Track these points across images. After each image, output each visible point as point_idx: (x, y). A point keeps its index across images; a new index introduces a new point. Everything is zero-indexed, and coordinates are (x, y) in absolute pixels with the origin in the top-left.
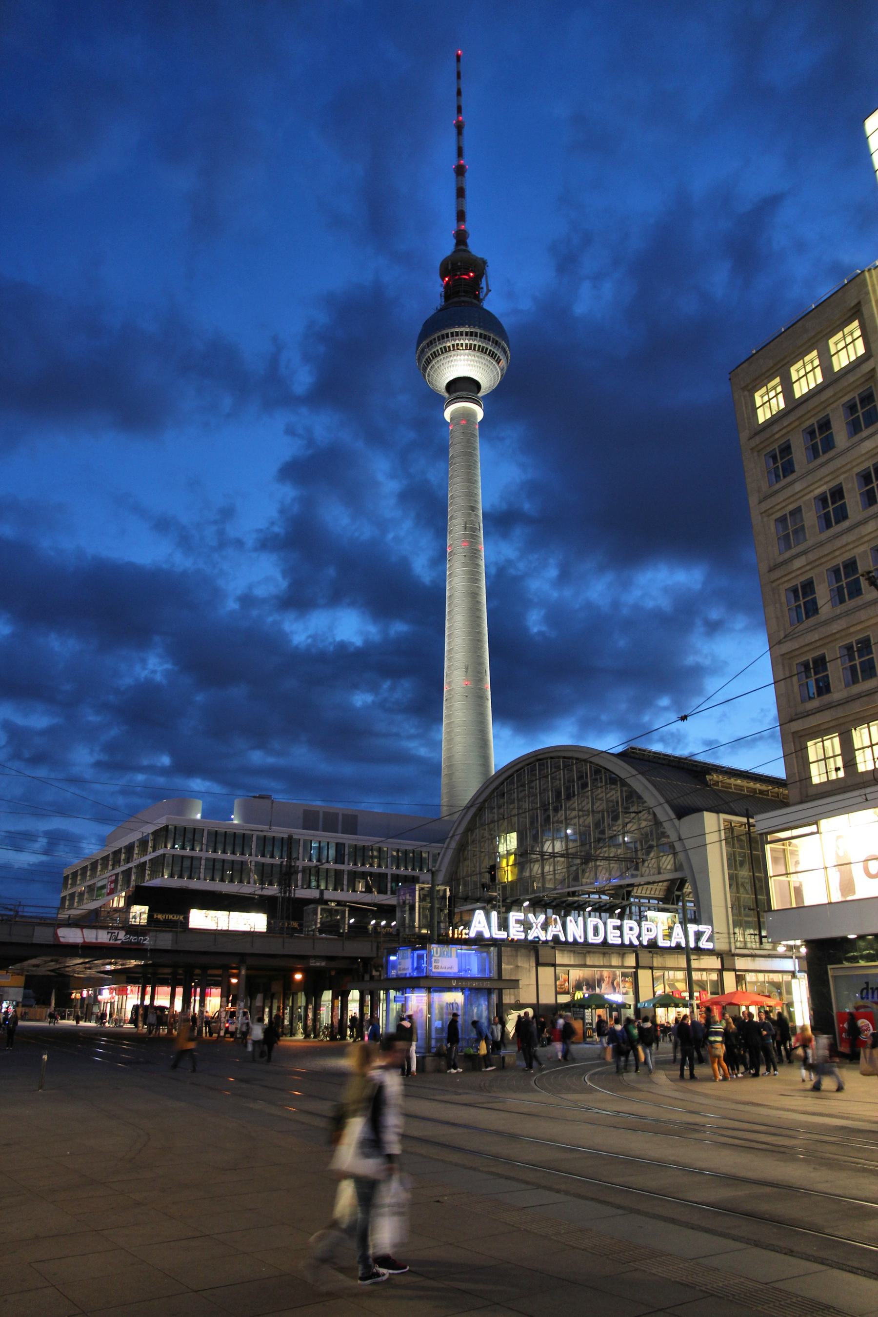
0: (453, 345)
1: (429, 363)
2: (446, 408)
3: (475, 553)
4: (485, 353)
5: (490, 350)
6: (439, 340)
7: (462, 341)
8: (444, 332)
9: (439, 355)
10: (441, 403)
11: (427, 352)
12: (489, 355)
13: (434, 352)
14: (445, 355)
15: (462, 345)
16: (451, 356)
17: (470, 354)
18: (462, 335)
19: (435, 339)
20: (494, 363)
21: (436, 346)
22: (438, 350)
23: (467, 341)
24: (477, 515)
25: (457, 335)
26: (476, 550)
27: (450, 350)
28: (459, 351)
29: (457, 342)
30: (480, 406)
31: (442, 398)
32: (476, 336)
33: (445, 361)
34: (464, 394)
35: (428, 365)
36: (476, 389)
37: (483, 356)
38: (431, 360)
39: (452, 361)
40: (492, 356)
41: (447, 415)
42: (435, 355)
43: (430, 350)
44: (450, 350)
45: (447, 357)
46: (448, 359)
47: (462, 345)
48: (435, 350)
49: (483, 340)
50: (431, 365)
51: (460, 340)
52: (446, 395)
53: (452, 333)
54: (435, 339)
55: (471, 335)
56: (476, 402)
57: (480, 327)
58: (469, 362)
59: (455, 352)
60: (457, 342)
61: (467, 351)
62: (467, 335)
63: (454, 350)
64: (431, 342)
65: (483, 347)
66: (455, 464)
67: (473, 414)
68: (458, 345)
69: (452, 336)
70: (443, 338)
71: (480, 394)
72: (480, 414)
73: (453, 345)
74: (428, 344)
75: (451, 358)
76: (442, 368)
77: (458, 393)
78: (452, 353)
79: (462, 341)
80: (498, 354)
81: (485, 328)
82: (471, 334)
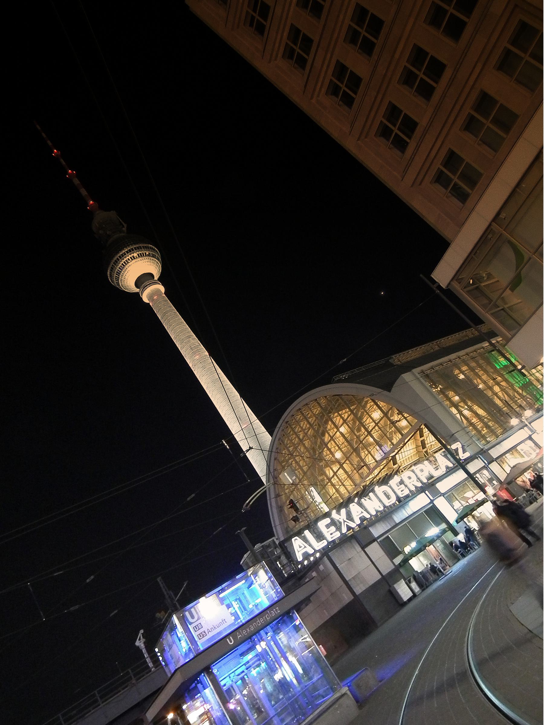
0: (124, 262)
8: (115, 258)
11: (113, 275)
19: (113, 265)
22: (118, 270)
23: (130, 256)
25: (123, 256)
27: (124, 266)
28: (130, 264)
31: (137, 294)
32: (133, 250)
34: (147, 283)
41: (145, 299)
42: (119, 273)
46: (127, 271)
53: (120, 257)
55: (130, 251)
56: (155, 283)
59: (128, 265)
62: (128, 253)
63: (126, 264)
64: (112, 268)
67: (159, 291)
68: (126, 260)
71: (156, 278)
72: (162, 289)
74: (111, 270)
81: (135, 244)
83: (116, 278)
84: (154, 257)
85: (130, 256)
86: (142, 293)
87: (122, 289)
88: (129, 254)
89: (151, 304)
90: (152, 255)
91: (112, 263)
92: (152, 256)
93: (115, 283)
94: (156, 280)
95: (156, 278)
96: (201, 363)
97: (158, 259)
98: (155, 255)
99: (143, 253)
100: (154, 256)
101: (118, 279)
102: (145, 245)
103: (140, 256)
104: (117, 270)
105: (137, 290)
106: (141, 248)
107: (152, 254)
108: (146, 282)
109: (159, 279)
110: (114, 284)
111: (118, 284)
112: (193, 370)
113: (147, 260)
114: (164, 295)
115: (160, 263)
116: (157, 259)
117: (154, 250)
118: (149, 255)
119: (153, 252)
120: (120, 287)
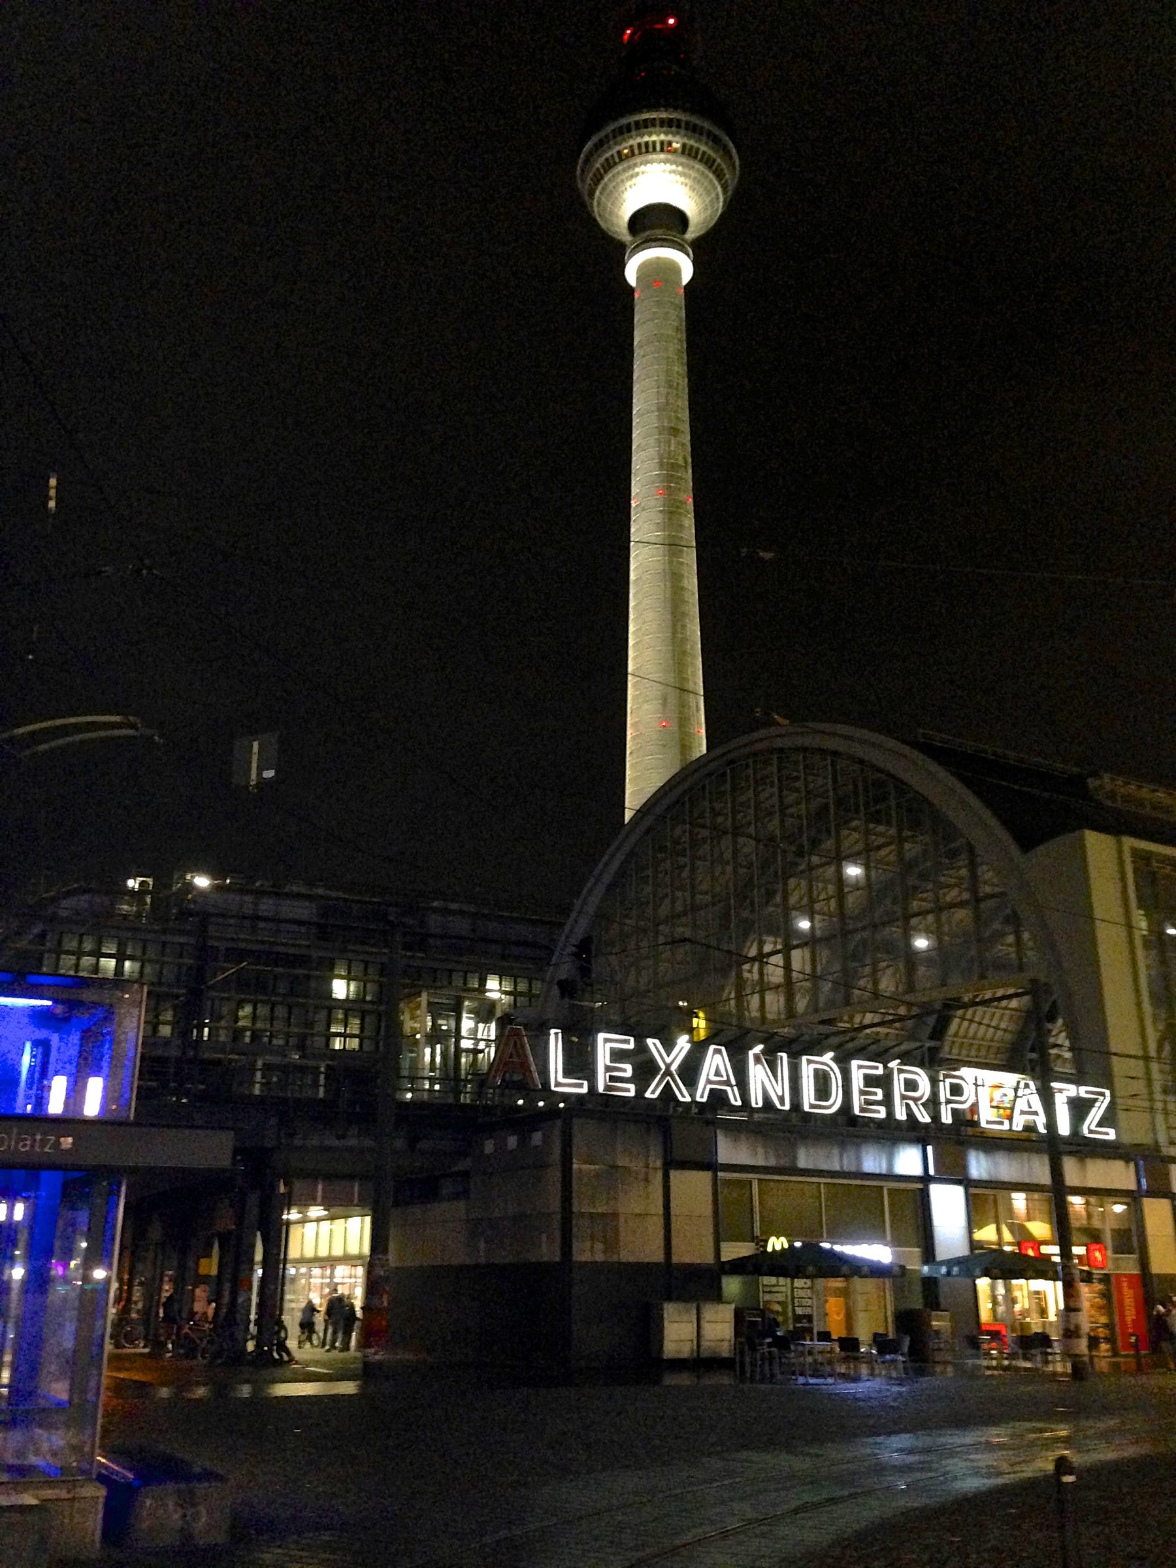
2: (630, 257)
3: (678, 507)
4: (695, 157)
6: (615, 137)
8: (624, 121)
10: (617, 254)
12: (701, 161)
14: (625, 165)
16: (635, 165)
18: (654, 125)
21: (610, 148)
26: (680, 502)
29: (646, 138)
30: (688, 255)
32: (679, 126)
33: (627, 175)
34: (659, 233)
37: (692, 162)
38: (602, 178)
41: (631, 274)
42: (609, 165)
43: (600, 156)
45: (629, 168)
46: (631, 172)
48: (608, 155)
49: (690, 133)
50: (603, 183)
51: (650, 134)
53: (637, 123)
54: (607, 136)
56: (681, 248)
60: (646, 138)
61: (662, 156)
63: (640, 153)
64: (601, 141)
66: (644, 356)
67: (675, 270)
70: (622, 133)
71: (690, 235)
72: (687, 271)
73: (639, 145)
75: (637, 170)
77: (648, 233)
78: (638, 160)
83: (595, 175)
85: (662, 137)
89: (636, 296)
90: (716, 169)
91: (610, 128)
95: (690, 235)
97: (725, 188)
100: (719, 174)
101: (598, 179)
102: (717, 131)
106: (701, 134)
108: (661, 231)
110: (583, 188)
111: (591, 194)
112: (633, 518)
113: (693, 174)
115: (725, 201)
117: (731, 157)
118: (708, 162)
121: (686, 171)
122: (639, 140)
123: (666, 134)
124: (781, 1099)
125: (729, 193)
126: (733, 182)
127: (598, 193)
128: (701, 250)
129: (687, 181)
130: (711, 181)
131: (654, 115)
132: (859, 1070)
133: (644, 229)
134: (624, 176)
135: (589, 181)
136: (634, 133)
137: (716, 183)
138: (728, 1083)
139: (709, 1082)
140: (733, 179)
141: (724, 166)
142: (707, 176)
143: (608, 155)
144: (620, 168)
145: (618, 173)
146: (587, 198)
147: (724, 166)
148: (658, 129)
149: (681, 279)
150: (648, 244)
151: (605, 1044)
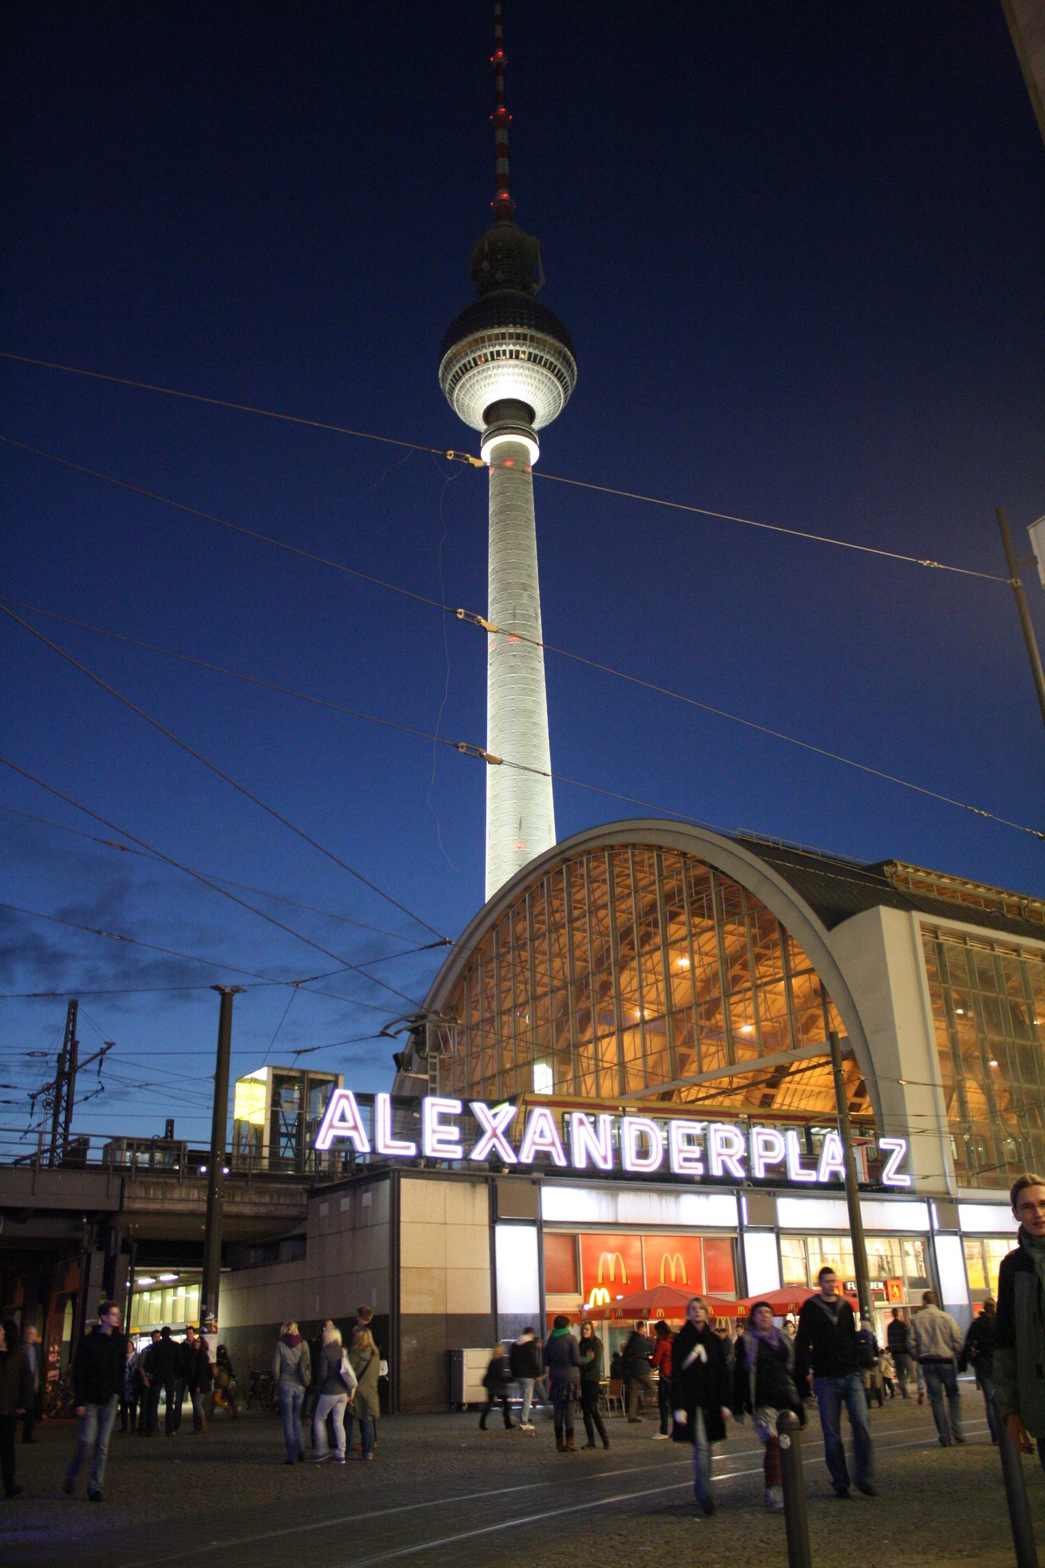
0: (492, 353)
1: (457, 381)
2: (484, 444)
5: (546, 359)
7: (504, 347)
8: (479, 335)
9: (471, 367)
10: (472, 441)
12: (545, 365)
13: (464, 365)
15: (504, 352)
16: (488, 369)
17: (517, 366)
20: (553, 378)
22: (469, 362)
23: (511, 347)
24: (531, 597)
25: (497, 339)
29: (497, 348)
30: (534, 440)
31: (478, 434)
32: (525, 339)
34: (510, 423)
35: (455, 384)
36: (528, 419)
37: (536, 368)
38: (460, 378)
39: (490, 376)
40: (549, 368)
42: (466, 369)
44: (487, 361)
45: (483, 371)
46: (485, 374)
47: (504, 352)
50: (460, 383)
51: (501, 345)
52: (481, 426)
56: (528, 434)
57: (530, 327)
58: (516, 377)
59: (495, 363)
60: (497, 348)
63: (493, 359)
65: (536, 356)
67: (524, 452)
68: (498, 352)
69: (490, 340)
71: (537, 425)
72: (534, 454)
73: (492, 353)
75: (490, 372)
76: (477, 387)
77: (500, 423)
78: (491, 364)
79: (504, 347)
80: (559, 366)
82: (518, 337)
83: (454, 376)
84: (559, 379)
85: (511, 347)
86: (491, 435)
87: (453, 404)
88: (511, 341)
92: (556, 375)
93: (447, 386)
94: (533, 430)
95: (537, 425)
96: (514, 656)
97: (565, 390)
98: (565, 378)
99: (542, 358)
100: (560, 377)
101: (457, 379)
103: (533, 359)
104: (467, 359)
105: (481, 426)
107: (559, 370)
108: (511, 421)
109: (542, 432)
112: (489, 662)
113: (538, 377)
114: (530, 470)
115: (565, 398)
116: (563, 386)
117: (570, 365)
118: (551, 368)
119: (564, 367)
120: (452, 400)
121: (531, 373)
122: (491, 349)
123: (515, 345)
124: (605, 1159)
125: (570, 392)
126: (572, 384)
127: (456, 391)
128: (545, 437)
129: (533, 382)
130: (553, 382)
131: (503, 330)
132: (680, 1128)
133: (498, 420)
134: (478, 378)
135: (449, 381)
136: (487, 344)
137: (558, 384)
138: (553, 1144)
139: (534, 1144)
140: (572, 379)
141: (563, 370)
142: (550, 378)
143: (465, 361)
144: (475, 371)
145: (474, 375)
146: (447, 395)
147: (563, 370)
148: (507, 341)
149: (529, 460)
150: (501, 431)
151: (433, 1107)
